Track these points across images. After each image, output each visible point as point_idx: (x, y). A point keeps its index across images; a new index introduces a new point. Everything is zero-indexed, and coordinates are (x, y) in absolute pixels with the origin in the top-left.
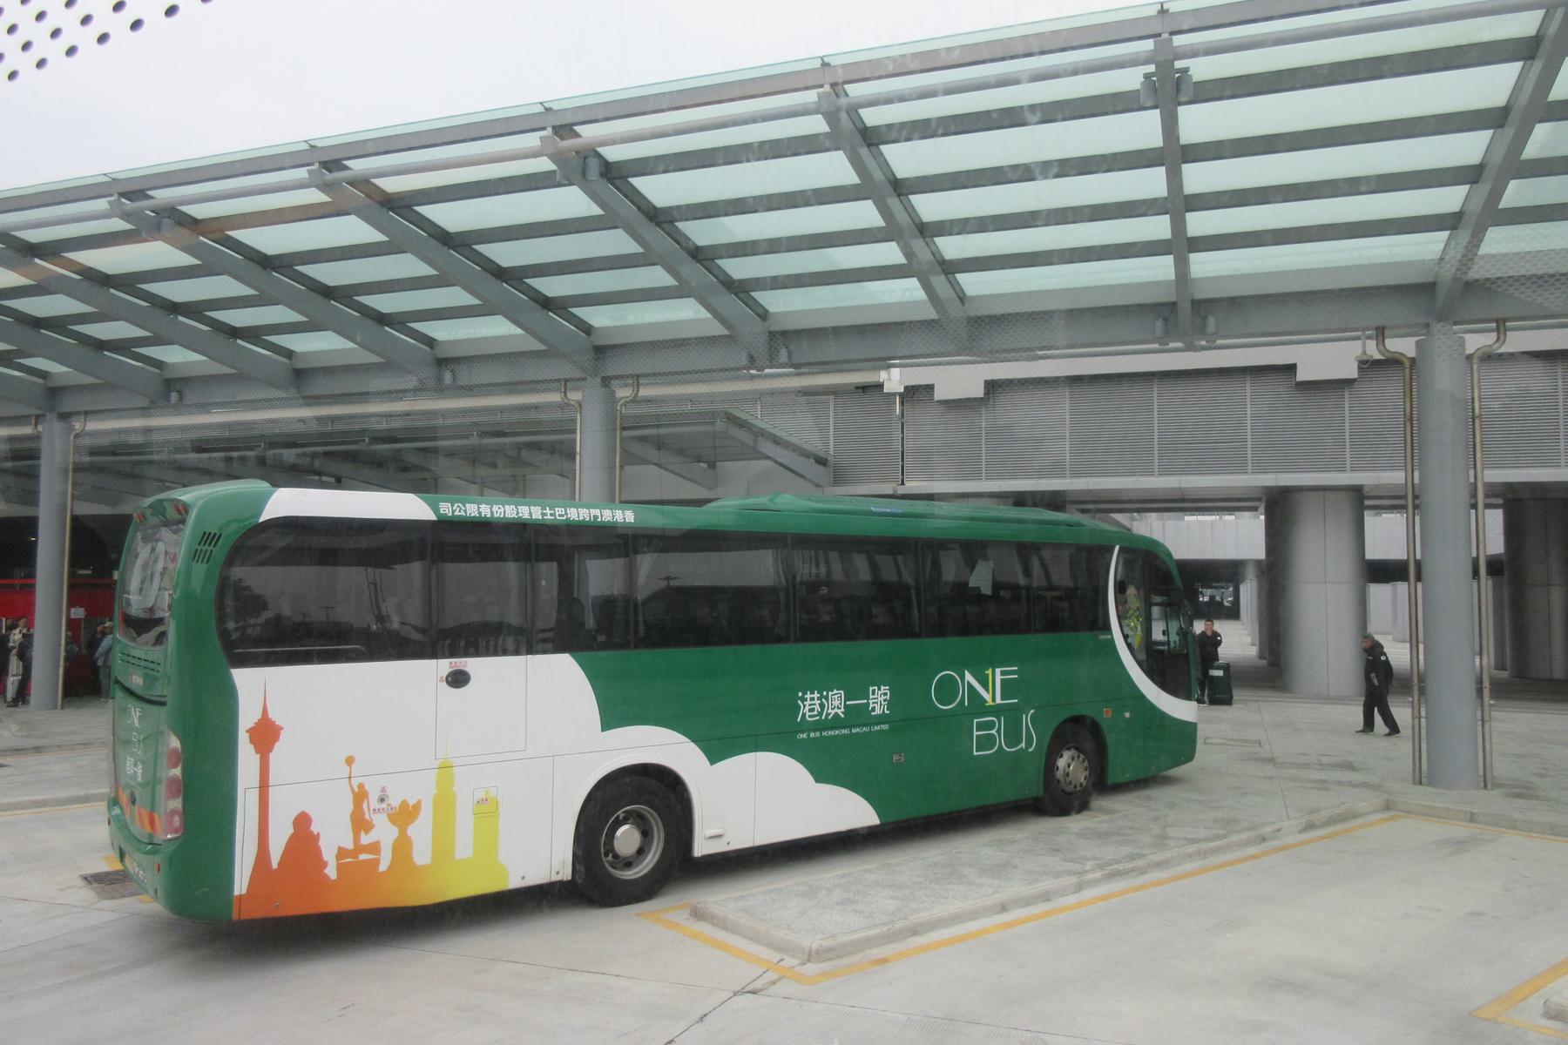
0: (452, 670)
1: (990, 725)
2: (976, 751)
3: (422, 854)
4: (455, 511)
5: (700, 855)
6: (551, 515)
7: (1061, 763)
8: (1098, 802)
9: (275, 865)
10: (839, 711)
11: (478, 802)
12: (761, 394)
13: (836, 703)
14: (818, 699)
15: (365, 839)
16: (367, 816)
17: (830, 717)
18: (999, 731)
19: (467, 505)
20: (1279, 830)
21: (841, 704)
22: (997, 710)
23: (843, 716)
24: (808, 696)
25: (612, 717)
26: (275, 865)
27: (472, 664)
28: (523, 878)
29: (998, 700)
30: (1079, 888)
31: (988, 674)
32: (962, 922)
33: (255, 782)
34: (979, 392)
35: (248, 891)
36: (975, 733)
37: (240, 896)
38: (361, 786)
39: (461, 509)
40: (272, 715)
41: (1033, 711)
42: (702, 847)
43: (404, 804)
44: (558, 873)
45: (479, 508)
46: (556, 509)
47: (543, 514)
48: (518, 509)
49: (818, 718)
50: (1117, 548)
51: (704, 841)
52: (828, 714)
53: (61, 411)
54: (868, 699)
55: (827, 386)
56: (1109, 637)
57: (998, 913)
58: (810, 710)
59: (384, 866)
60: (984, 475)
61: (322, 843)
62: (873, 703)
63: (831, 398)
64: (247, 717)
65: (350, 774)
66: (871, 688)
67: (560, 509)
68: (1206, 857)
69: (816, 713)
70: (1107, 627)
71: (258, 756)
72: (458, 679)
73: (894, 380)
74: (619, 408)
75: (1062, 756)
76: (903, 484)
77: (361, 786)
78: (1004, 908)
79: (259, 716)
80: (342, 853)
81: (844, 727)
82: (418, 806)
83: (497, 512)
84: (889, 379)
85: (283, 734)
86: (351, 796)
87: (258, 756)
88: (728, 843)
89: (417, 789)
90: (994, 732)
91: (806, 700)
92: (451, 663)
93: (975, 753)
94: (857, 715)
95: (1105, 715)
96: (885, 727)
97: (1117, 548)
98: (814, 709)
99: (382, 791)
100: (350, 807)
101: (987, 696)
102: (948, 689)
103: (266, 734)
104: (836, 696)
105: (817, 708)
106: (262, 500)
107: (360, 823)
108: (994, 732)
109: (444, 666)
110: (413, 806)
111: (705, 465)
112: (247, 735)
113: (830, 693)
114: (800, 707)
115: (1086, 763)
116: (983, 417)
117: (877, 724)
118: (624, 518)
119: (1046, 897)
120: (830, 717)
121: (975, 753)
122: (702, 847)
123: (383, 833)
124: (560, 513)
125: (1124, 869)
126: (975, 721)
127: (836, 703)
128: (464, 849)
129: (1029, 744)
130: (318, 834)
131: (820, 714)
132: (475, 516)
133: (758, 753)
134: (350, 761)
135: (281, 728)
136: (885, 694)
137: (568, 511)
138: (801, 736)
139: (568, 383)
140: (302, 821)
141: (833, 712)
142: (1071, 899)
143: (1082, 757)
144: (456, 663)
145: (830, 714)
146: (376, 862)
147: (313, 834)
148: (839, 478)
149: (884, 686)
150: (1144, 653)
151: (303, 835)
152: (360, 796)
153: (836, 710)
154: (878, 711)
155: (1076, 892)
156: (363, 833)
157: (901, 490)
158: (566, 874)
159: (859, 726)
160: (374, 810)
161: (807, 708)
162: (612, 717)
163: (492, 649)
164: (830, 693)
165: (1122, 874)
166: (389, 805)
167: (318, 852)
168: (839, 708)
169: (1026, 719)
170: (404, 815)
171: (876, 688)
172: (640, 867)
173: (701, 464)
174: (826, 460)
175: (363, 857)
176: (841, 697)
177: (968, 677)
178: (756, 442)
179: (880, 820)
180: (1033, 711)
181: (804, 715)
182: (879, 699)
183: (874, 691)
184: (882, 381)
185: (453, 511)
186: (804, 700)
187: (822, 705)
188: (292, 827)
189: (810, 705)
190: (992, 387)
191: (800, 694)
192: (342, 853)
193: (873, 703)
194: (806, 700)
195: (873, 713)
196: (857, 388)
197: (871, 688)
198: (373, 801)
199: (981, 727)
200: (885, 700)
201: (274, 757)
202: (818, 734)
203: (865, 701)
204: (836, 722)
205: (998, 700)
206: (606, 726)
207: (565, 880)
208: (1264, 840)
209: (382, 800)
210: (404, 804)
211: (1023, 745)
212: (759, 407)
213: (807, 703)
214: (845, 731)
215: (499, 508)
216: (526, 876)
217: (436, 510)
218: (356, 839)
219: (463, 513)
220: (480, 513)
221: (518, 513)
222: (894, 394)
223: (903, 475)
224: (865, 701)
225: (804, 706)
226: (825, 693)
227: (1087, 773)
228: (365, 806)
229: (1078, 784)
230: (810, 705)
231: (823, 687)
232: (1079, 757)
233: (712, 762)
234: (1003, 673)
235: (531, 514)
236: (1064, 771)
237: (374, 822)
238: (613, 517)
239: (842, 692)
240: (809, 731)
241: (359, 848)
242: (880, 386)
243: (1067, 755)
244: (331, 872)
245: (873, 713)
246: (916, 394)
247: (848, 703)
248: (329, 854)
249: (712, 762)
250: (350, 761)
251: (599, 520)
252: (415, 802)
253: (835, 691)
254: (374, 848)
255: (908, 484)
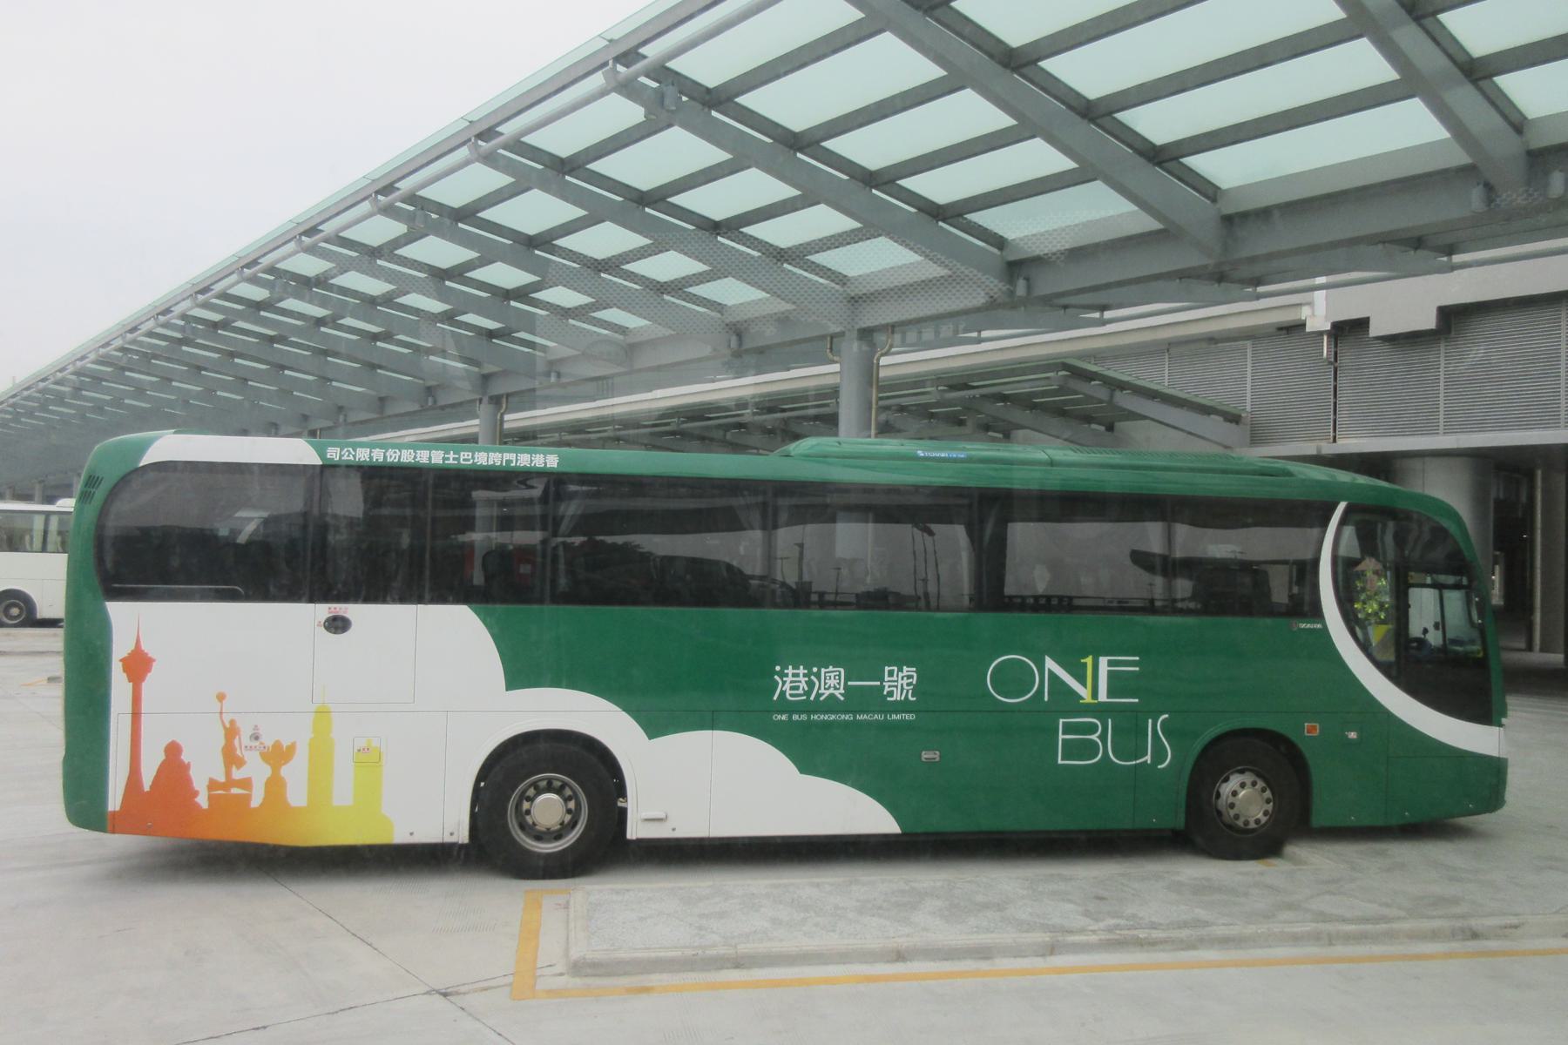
0: (331, 615)
1: (1091, 729)
2: (1062, 759)
3: (297, 796)
4: (343, 456)
5: (634, 838)
6: (454, 459)
7: (1226, 789)
8: (1298, 850)
9: (147, 788)
10: (837, 693)
11: (359, 750)
12: (1169, 344)
13: (832, 682)
14: (805, 675)
15: (237, 774)
16: (238, 752)
17: (822, 699)
18: (1103, 737)
19: (403, 451)
20: (1516, 927)
21: (839, 684)
22: (1099, 710)
23: (842, 698)
24: (790, 671)
25: (520, 674)
26: (147, 788)
27: (351, 610)
28: (411, 834)
29: (1103, 696)
30: (1052, 949)
31: (1085, 664)
32: (825, 963)
33: (128, 707)
34: (1429, 322)
35: (121, 807)
36: (1061, 737)
37: (114, 813)
38: (232, 722)
39: (350, 453)
40: (145, 647)
41: (1167, 716)
42: (636, 830)
43: (277, 745)
44: (452, 834)
45: (371, 452)
46: (462, 454)
47: (444, 459)
48: (416, 453)
49: (804, 698)
50: (1342, 506)
51: (640, 823)
52: (819, 695)
53: (491, 394)
54: (882, 680)
55: (1239, 330)
56: (1319, 626)
57: (888, 962)
58: (792, 688)
59: (255, 802)
60: (1441, 427)
61: (193, 773)
62: (889, 687)
63: (1249, 343)
64: (120, 648)
65: (221, 709)
66: (887, 669)
67: (466, 453)
68: (1331, 944)
69: (801, 691)
70: (1316, 612)
71: (131, 684)
72: (338, 625)
73: (1319, 312)
74: (875, 362)
75: (1226, 780)
76: (1335, 441)
77: (232, 722)
78: (900, 956)
79: (132, 647)
80: (213, 785)
81: (846, 712)
82: (292, 748)
83: (391, 457)
84: (1313, 315)
85: (155, 666)
86: (222, 732)
87: (131, 684)
88: (674, 829)
89: (296, 732)
90: (1094, 737)
91: (787, 675)
92: (330, 608)
93: (1060, 762)
94: (856, 700)
95: (1309, 732)
96: (910, 717)
97: (1342, 506)
98: (799, 687)
99: (254, 729)
100: (222, 742)
101: (1085, 693)
102: (1014, 679)
103: (138, 665)
104: (832, 675)
105: (803, 686)
106: (143, 447)
107: (231, 758)
108: (1094, 737)
109: (323, 610)
110: (288, 747)
111: (1102, 428)
112: (121, 664)
113: (823, 670)
114: (778, 683)
115: (1268, 794)
116: (1442, 355)
117: (896, 712)
118: (545, 463)
119: (984, 953)
120: (822, 699)
121: (1060, 762)
122: (636, 830)
123: (256, 770)
124: (466, 457)
125: (1145, 938)
126: (1061, 721)
127: (832, 682)
128: (343, 792)
129: (1159, 754)
130: (189, 764)
131: (808, 693)
132: (365, 461)
133: (717, 733)
134: (221, 697)
135: (154, 660)
136: (909, 677)
137: (476, 456)
138: (779, 717)
139: (835, 340)
140: (173, 750)
141: (827, 693)
142: (1039, 962)
143: (1261, 784)
144: (335, 608)
145: (823, 694)
146: (248, 798)
147: (184, 763)
148: (1256, 439)
149: (908, 667)
150: (1392, 650)
151: (174, 766)
152: (231, 732)
153: (832, 691)
154: (897, 696)
155: (1043, 955)
156: (234, 769)
157: (1328, 449)
158: (462, 835)
159: (867, 712)
160: (246, 747)
161: (787, 686)
162: (520, 674)
163: (427, 596)
164: (823, 670)
165: (1141, 944)
166: (261, 743)
167: (188, 780)
168: (835, 688)
169: (1155, 726)
170: (278, 755)
171: (896, 669)
172: (567, 839)
173: (1094, 426)
174: (1240, 416)
175: (235, 791)
176: (839, 676)
177: (1050, 664)
178: (1112, 396)
179: (901, 829)
180: (1167, 716)
181: (783, 693)
182: (899, 682)
183: (891, 674)
184: (1303, 318)
185: (341, 456)
186: (782, 675)
187: (810, 684)
188: (163, 753)
189: (791, 682)
190: (1454, 318)
191: (778, 668)
192: (213, 785)
193: (889, 687)
194: (787, 675)
195: (889, 699)
196: (1280, 329)
197: (887, 669)
198: (245, 738)
199: (1069, 729)
200: (908, 685)
201: (147, 686)
202: (804, 717)
203: (878, 683)
204: (831, 705)
205: (1103, 696)
206: (509, 687)
207: (460, 842)
208: (1475, 935)
209: (257, 738)
210: (277, 745)
211: (1148, 758)
212: (1167, 357)
213: (788, 680)
214: (847, 717)
215: (395, 452)
216: (415, 833)
217: (322, 455)
218: (228, 773)
219: (351, 458)
220: (371, 458)
221: (415, 457)
222: (1321, 333)
223: (1335, 430)
224: (878, 683)
225: (784, 683)
226: (815, 670)
227: (1270, 807)
228: (236, 742)
229: (1252, 821)
230: (791, 682)
231: (815, 660)
232: (1254, 784)
233: (650, 739)
234: (1110, 663)
235: (430, 458)
236: (1228, 797)
237: (246, 759)
238: (531, 461)
239: (842, 670)
240: (791, 713)
241: (230, 783)
242: (1303, 325)
243: (1235, 781)
244: (203, 800)
245: (889, 699)
246: (1349, 331)
247: (849, 683)
248: (199, 782)
249: (650, 739)
250: (221, 697)
251: (513, 465)
252: (289, 744)
253: (831, 668)
254: (246, 783)
255: (1340, 442)
